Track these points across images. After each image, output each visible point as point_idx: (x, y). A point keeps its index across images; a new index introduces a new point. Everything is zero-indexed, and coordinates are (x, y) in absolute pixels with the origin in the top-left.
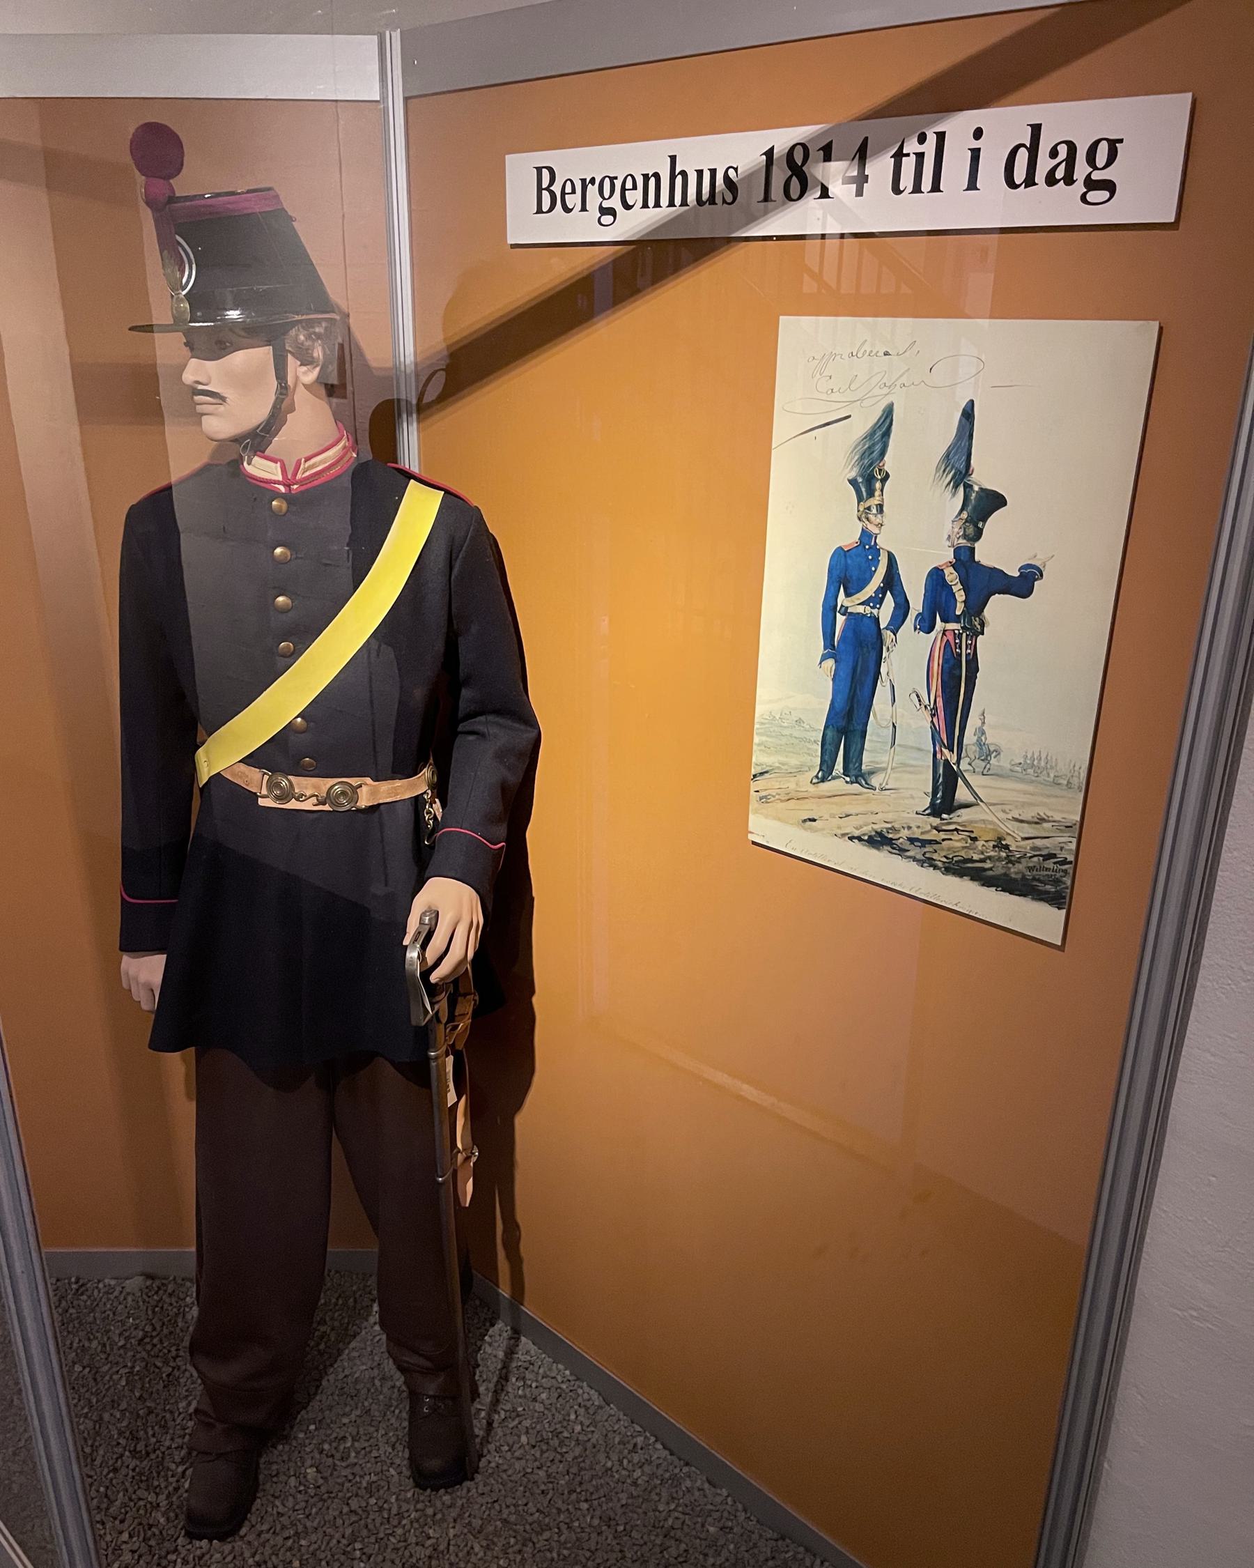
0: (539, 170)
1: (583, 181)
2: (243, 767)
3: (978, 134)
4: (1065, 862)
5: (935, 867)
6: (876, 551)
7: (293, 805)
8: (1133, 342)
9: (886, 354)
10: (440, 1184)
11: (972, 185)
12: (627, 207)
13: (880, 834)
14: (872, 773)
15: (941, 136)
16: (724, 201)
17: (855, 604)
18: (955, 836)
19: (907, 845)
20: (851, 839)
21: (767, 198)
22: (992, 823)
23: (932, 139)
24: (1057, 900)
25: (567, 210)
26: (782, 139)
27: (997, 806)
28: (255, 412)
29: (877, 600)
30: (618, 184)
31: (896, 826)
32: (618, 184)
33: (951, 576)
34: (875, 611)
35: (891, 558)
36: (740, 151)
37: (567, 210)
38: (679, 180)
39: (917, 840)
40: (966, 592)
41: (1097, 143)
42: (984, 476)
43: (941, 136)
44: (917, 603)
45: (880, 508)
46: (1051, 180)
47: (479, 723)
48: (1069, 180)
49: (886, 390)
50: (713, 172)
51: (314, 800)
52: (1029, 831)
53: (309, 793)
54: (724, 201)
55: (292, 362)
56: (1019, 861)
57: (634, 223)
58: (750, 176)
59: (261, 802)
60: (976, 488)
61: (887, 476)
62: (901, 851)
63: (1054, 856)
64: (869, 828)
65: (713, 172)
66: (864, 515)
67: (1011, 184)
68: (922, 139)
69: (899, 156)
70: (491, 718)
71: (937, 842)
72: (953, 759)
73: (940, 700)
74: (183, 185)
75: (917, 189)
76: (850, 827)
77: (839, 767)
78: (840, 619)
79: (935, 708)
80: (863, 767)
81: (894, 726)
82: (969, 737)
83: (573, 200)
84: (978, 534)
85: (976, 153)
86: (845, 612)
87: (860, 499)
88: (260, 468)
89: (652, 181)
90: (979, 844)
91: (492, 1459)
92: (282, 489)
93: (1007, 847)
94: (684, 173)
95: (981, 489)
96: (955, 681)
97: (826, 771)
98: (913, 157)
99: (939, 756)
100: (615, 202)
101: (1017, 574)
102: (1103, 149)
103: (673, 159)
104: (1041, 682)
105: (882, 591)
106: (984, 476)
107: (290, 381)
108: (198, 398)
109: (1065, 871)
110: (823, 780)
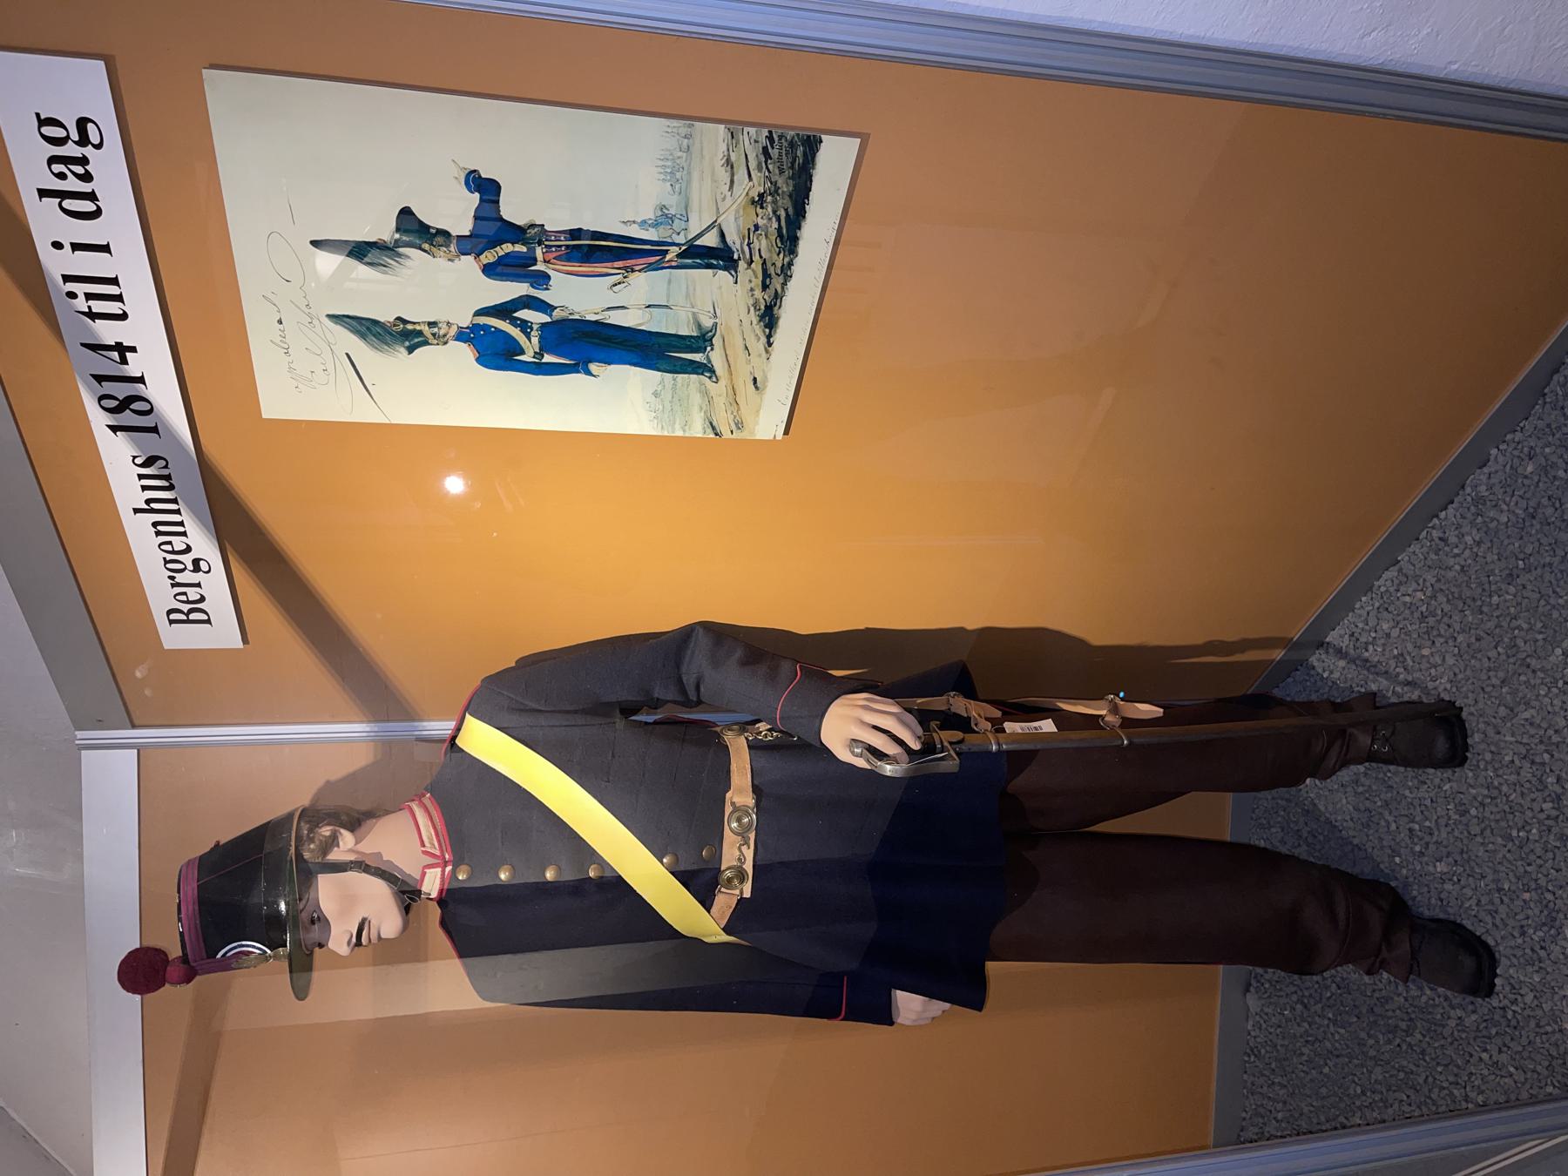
0: (171, 622)
2: (713, 910)
3: (58, 245)
4: (770, 137)
5: (790, 264)
6: (475, 328)
7: (749, 867)
8: (225, 94)
9: (280, 322)
10: (1131, 743)
11: (105, 249)
12: (188, 549)
13: (762, 318)
14: (699, 326)
16: (166, 467)
17: (530, 347)
18: (756, 245)
19: (771, 291)
20: (770, 344)
21: (154, 430)
22: (737, 211)
23: (71, 287)
24: (811, 144)
25: (202, 599)
26: (99, 420)
28: (379, 890)
29: (525, 326)
30: (169, 557)
31: (751, 302)
32: (169, 557)
33: (489, 257)
35: (479, 313)
36: (118, 456)
37: (202, 599)
38: (154, 506)
39: (764, 282)
41: (43, 137)
42: (386, 230)
43: (67, 278)
45: (432, 324)
46: (87, 177)
47: (689, 680)
48: (83, 161)
49: (315, 322)
51: (744, 848)
52: (741, 174)
53: (737, 852)
54: (166, 467)
55: (335, 856)
56: (775, 184)
57: (203, 544)
59: (747, 895)
60: (397, 236)
61: (399, 319)
62: (778, 297)
63: (765, 150)
65: (141, 477)
66: (442, 340)
67: (97, 213)
68: (72, 295)
69: (93, 316)
70: (684, 669)
71: (764, 263)
72: (674, 251)
73: (617, 264)
74: (175, 951)
75: (119, 298)
76: (758, 346)
77: (697, 357)
78: (548, 358)
79: (625, 268)
82: (650, 235)
83: (193, 594)
84: (446, 234)
85: (76, 247)
86: (539, 355)
87: (426, 343)
88: (432, 884)
89: (161, 528)
90: (761, 222)
91: (1442, 687)
92: (449, 868)
93: (761, 196)
94: (148, 502)
95: (398, 230)
97: (705, 369)
98: (91, 303)
100: (187, 559)
101: (477, 195)
102: (50, 131)
103: (136, 511)
104: (585, 169)
105: (514, 322)
106: (386, 230)
107: (352, 857)
108: (364, 940)
109: (780, 137)
110: (712, 371)
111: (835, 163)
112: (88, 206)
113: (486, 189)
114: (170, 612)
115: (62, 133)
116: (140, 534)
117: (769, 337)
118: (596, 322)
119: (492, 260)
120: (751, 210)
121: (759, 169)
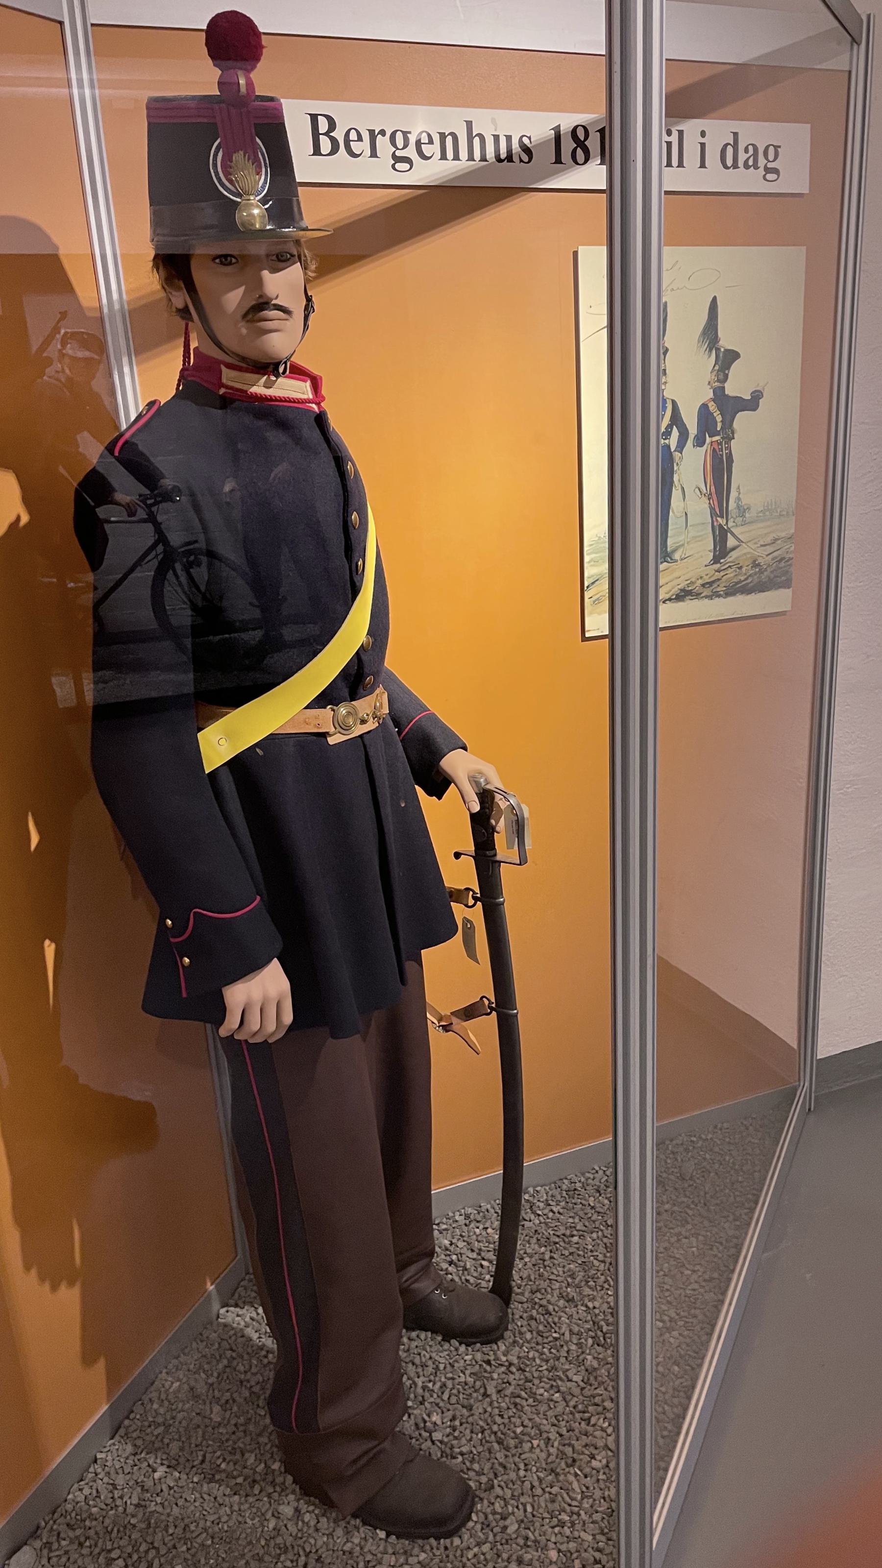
0: (314, 118)
1: (372, 132)
5: (719, 596)
8: (796, 255)
11: (703, 165)
13: (682, 590)
14: (674, 551)
15: (681, 133)
16: (521, 161)
18: (730, 570)
21: (558, 161)
22: (749, 553)
23: (675, 134)
24: (787, 584)
26: (567, 121)
27: (750, 542)
30: (412, 139)
31: (693, 580)
33: (712, 407)
34: (667, 441)
35: (674, 403)
38: (476, 141)
39: (707, 583)
40: (722, 413)
42: (726, 342)
43: (681, 133)
44: (693, 430)
48: (756, 167)
50: (509, 138)
52: (770, 549)
56: (766, 570)
57: (429, 171)
58: (542, 144)
60: (722, 350)
61: (667, 350)
62: (697, 596)
63: (784, 558)
64: (676, 589)
65: (509, 138)
67: (726, 167)
71: (719, 580)
73: (713, 487)
79: (711, 494)
80: (669, 550)
81: (686, 514)
82: (732, 505)
85: (703, 145)
89: (449, 140)
90: (744, 570)
93: (759, 565)
95: (726, 351)
96: (720, 470)
99: (715, 524)
100: (411, 152)
101: (749, 398)
102: (771, 150)
103: (469, 124)
105: (670, 427)
106: (726, 342)
111: (775, 601)
112: (729, 162)
113: (752, 404)
115: (771, 158)
116: (453, 119)
117: (670, 599)
118: (672, 482)
119: (711, 409)
120: (750, 561)
121: (773, 559)
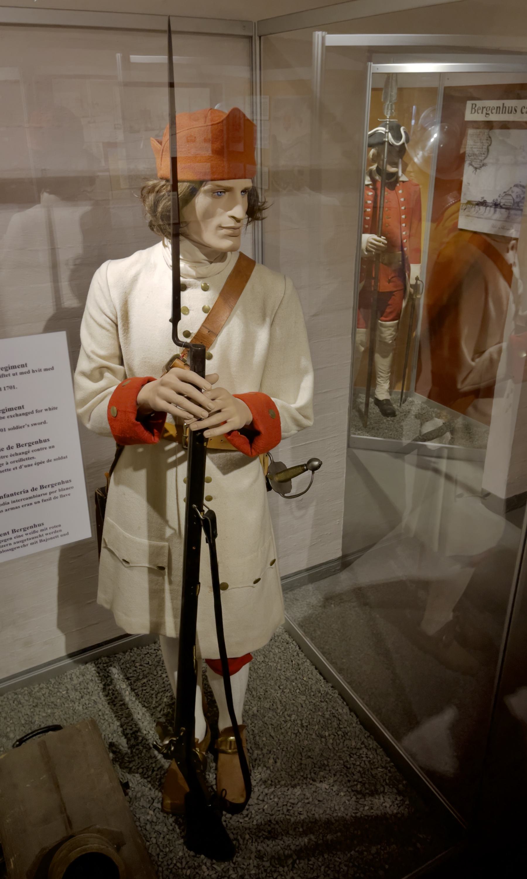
0: (473, 104)
25: (478, 113)
38: (504, 109)
65: (512, 107)
94: (506, 107)
100: (490, 112)
103: (503, 104)
114: (476, 105)
